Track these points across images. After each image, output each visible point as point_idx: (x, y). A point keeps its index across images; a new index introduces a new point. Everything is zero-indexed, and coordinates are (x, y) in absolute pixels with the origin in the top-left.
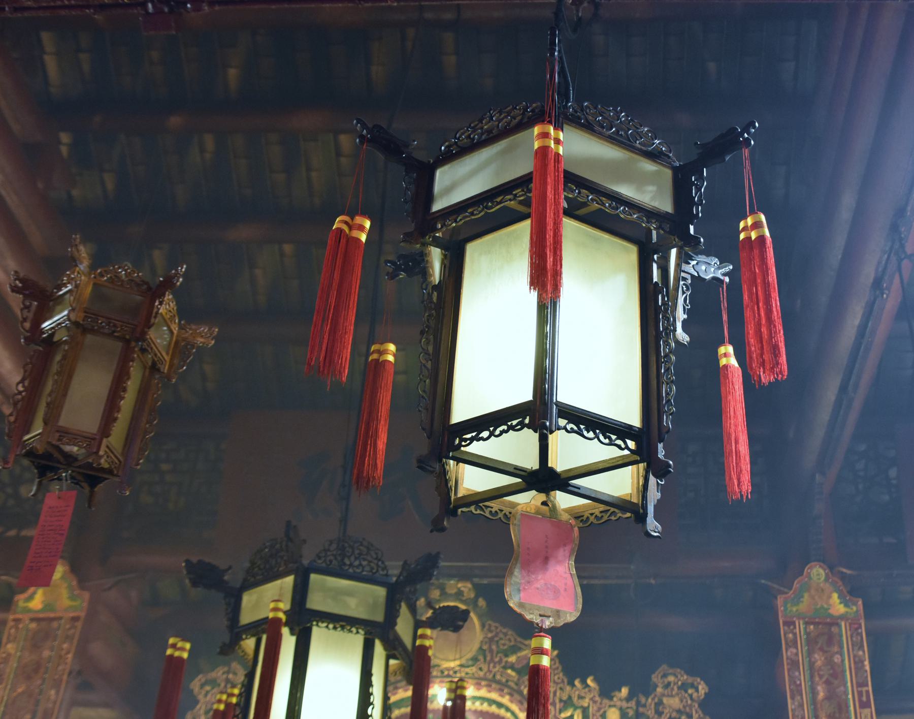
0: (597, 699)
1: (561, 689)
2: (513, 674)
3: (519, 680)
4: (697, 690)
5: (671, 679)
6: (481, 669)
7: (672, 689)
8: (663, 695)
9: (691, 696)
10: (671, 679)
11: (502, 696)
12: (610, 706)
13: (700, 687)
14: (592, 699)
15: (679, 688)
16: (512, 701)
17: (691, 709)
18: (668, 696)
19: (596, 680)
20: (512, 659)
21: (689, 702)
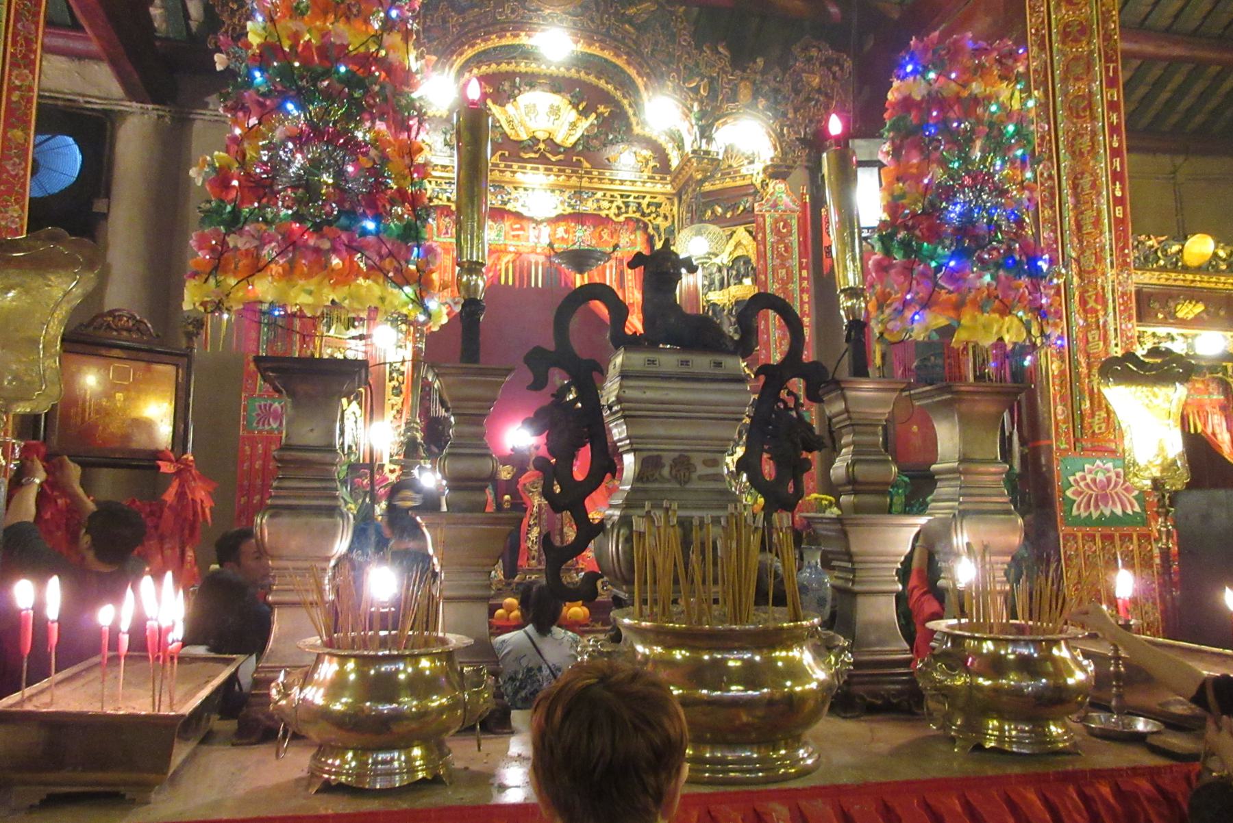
0: (729, 69)
1: (688, 53)
2: (632, 30)
3: (637, 37)
4: (842, 69)
5: (814, 52)
6: (592, 20)
7: (814, 64)
8: (804, 71)
9: (834, 74)
10: (814, 52)
11: (618, 56)
12: (742, 79)
13: (846, 65)
14: (722, 69)
15: (821, 64)
16: (629, 63)
17: (832, 89)
18: (809, 73)
19: (728, 47)
20: (631, 11)
21: (832, 81)
